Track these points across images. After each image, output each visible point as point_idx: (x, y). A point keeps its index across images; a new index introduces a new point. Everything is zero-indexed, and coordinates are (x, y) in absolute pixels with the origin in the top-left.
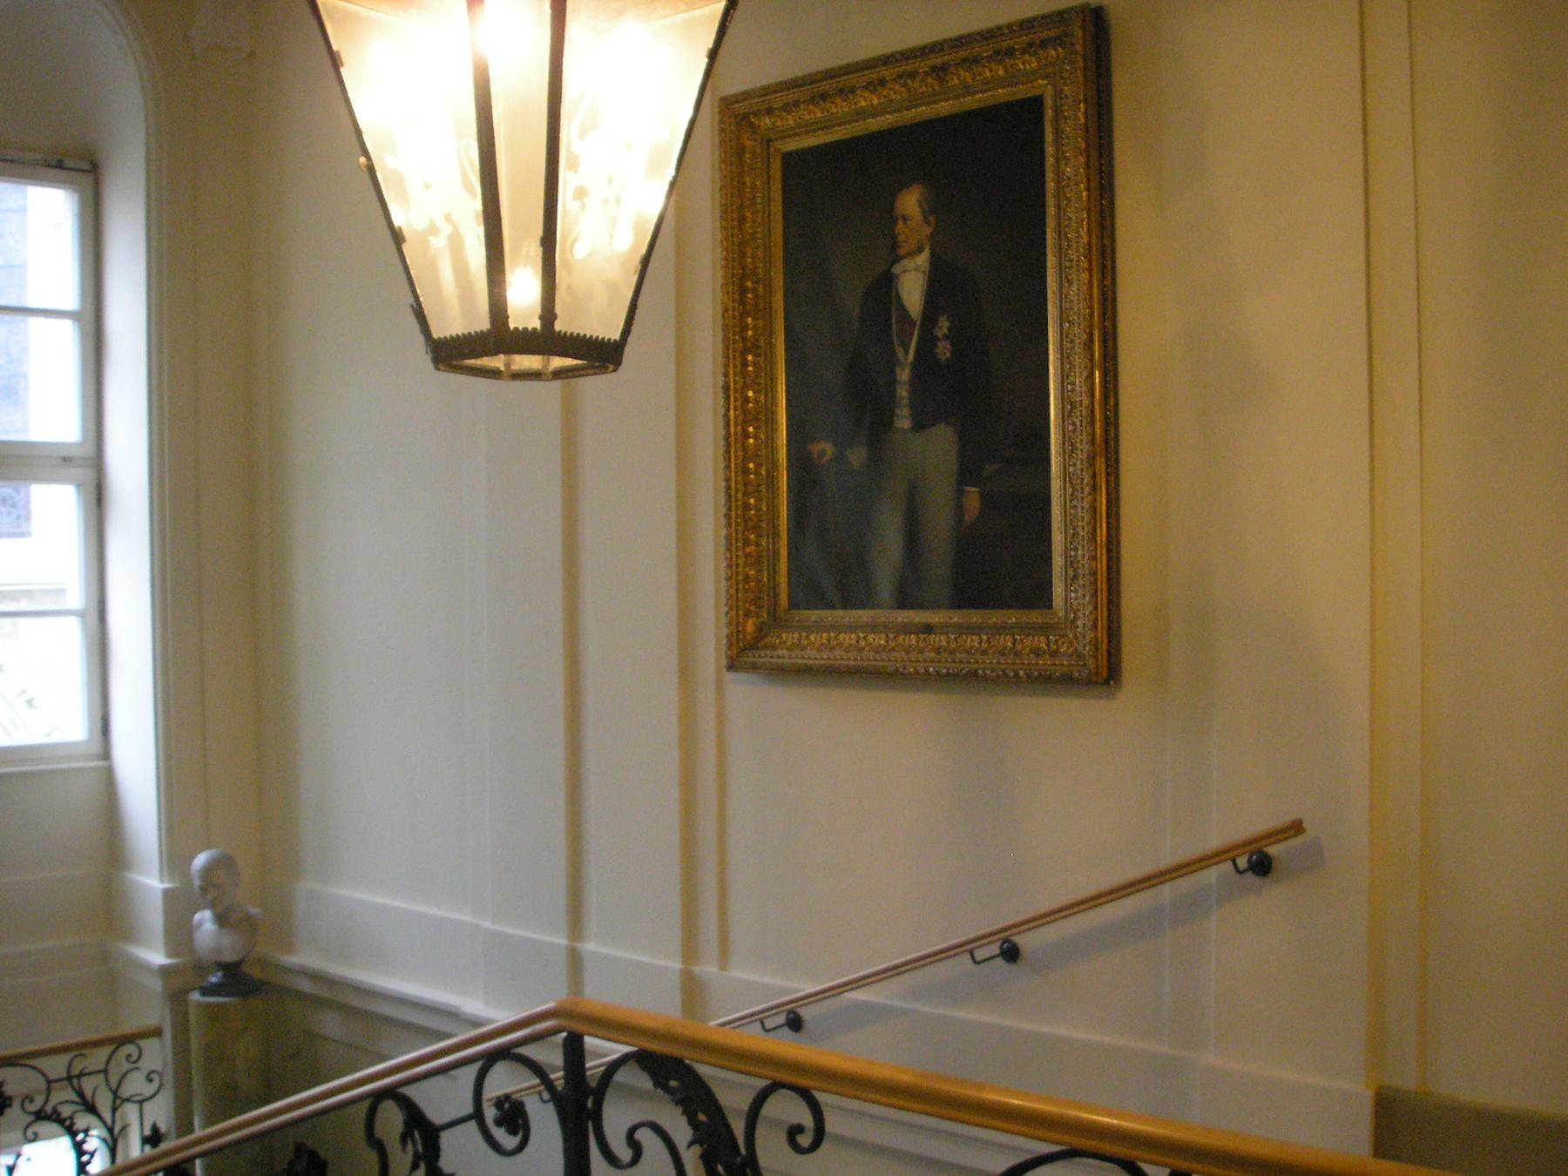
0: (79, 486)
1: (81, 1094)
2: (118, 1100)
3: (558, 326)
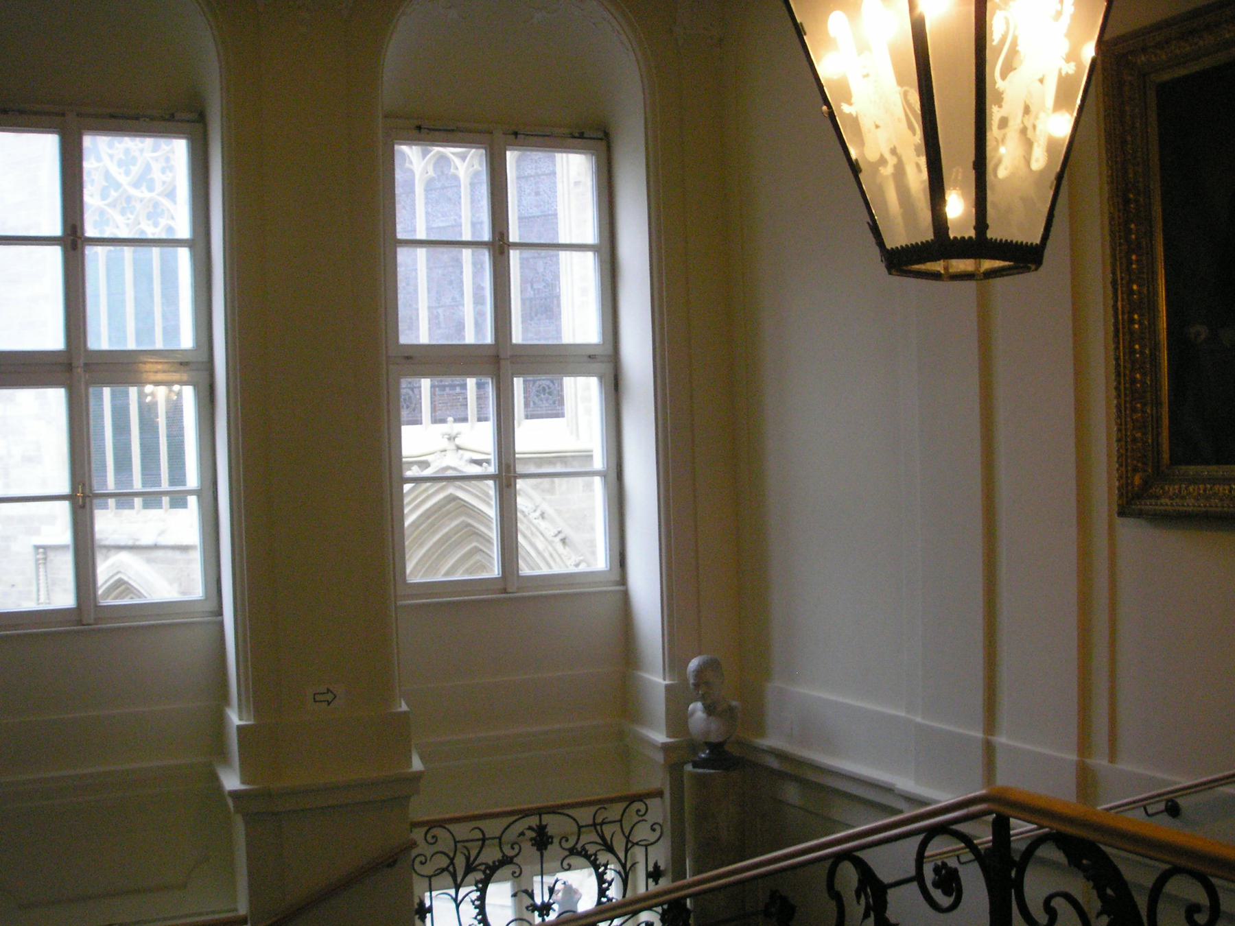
0: (601, 378)
1: (602, 837)
2: (629, 844)
3: (990, 234)
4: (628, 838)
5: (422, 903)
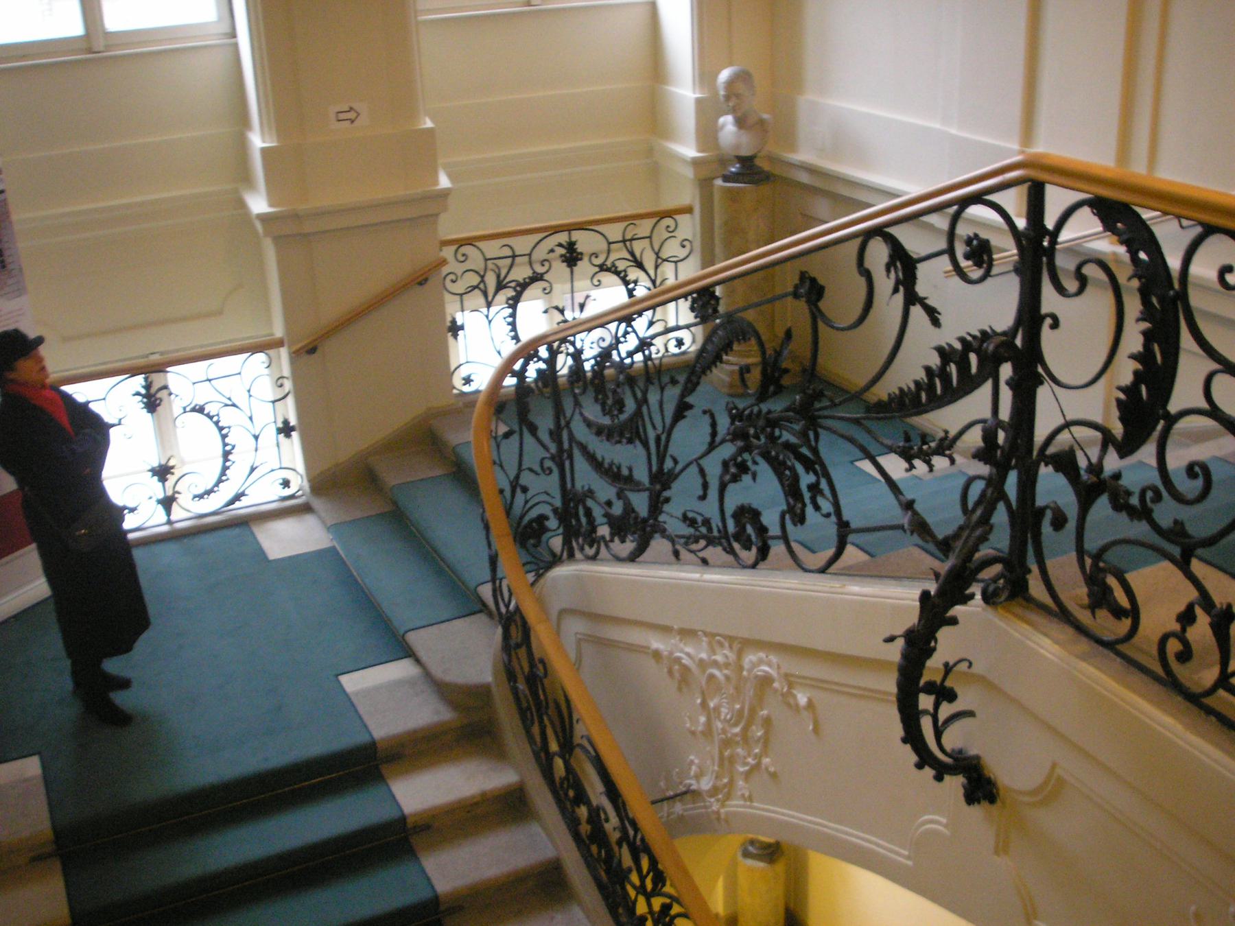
1: (632, 254)
2: (659, 260)
4: (657, 254)
5: (454, 321)
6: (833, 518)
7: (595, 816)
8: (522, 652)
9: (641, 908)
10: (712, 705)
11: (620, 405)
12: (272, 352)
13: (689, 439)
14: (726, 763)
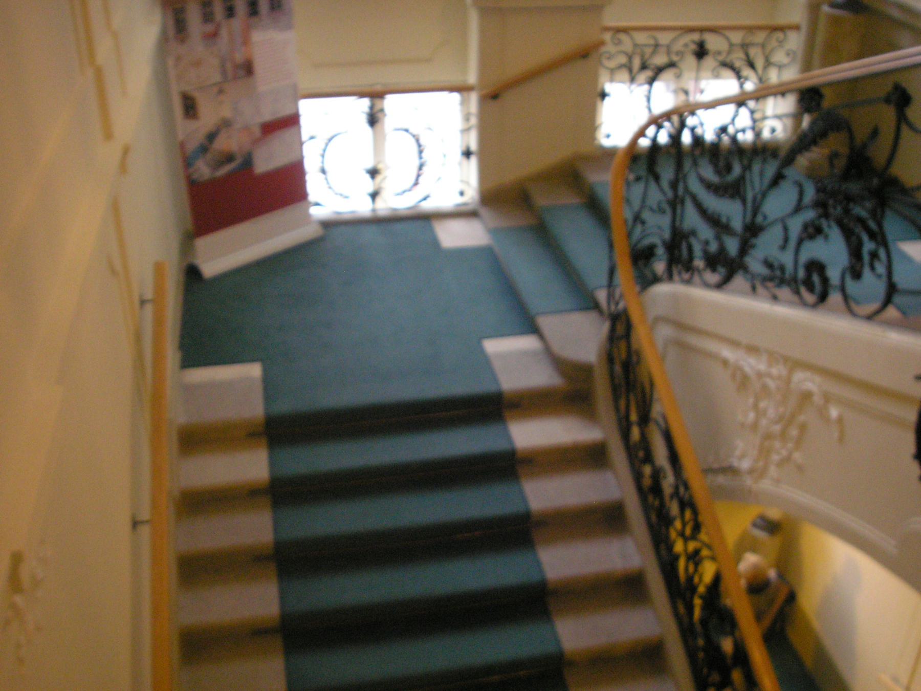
1: (747, 55)
2: (768, 64)
6: (884, 279)
7: (657, 475)
8: (623, 345)
9: (679, 547)
10: (762, 405)
11: (729, 168)
12: (465, 94)
13: (778, 204)
14: (764, 452)
